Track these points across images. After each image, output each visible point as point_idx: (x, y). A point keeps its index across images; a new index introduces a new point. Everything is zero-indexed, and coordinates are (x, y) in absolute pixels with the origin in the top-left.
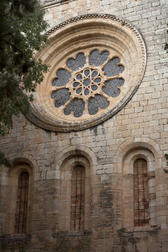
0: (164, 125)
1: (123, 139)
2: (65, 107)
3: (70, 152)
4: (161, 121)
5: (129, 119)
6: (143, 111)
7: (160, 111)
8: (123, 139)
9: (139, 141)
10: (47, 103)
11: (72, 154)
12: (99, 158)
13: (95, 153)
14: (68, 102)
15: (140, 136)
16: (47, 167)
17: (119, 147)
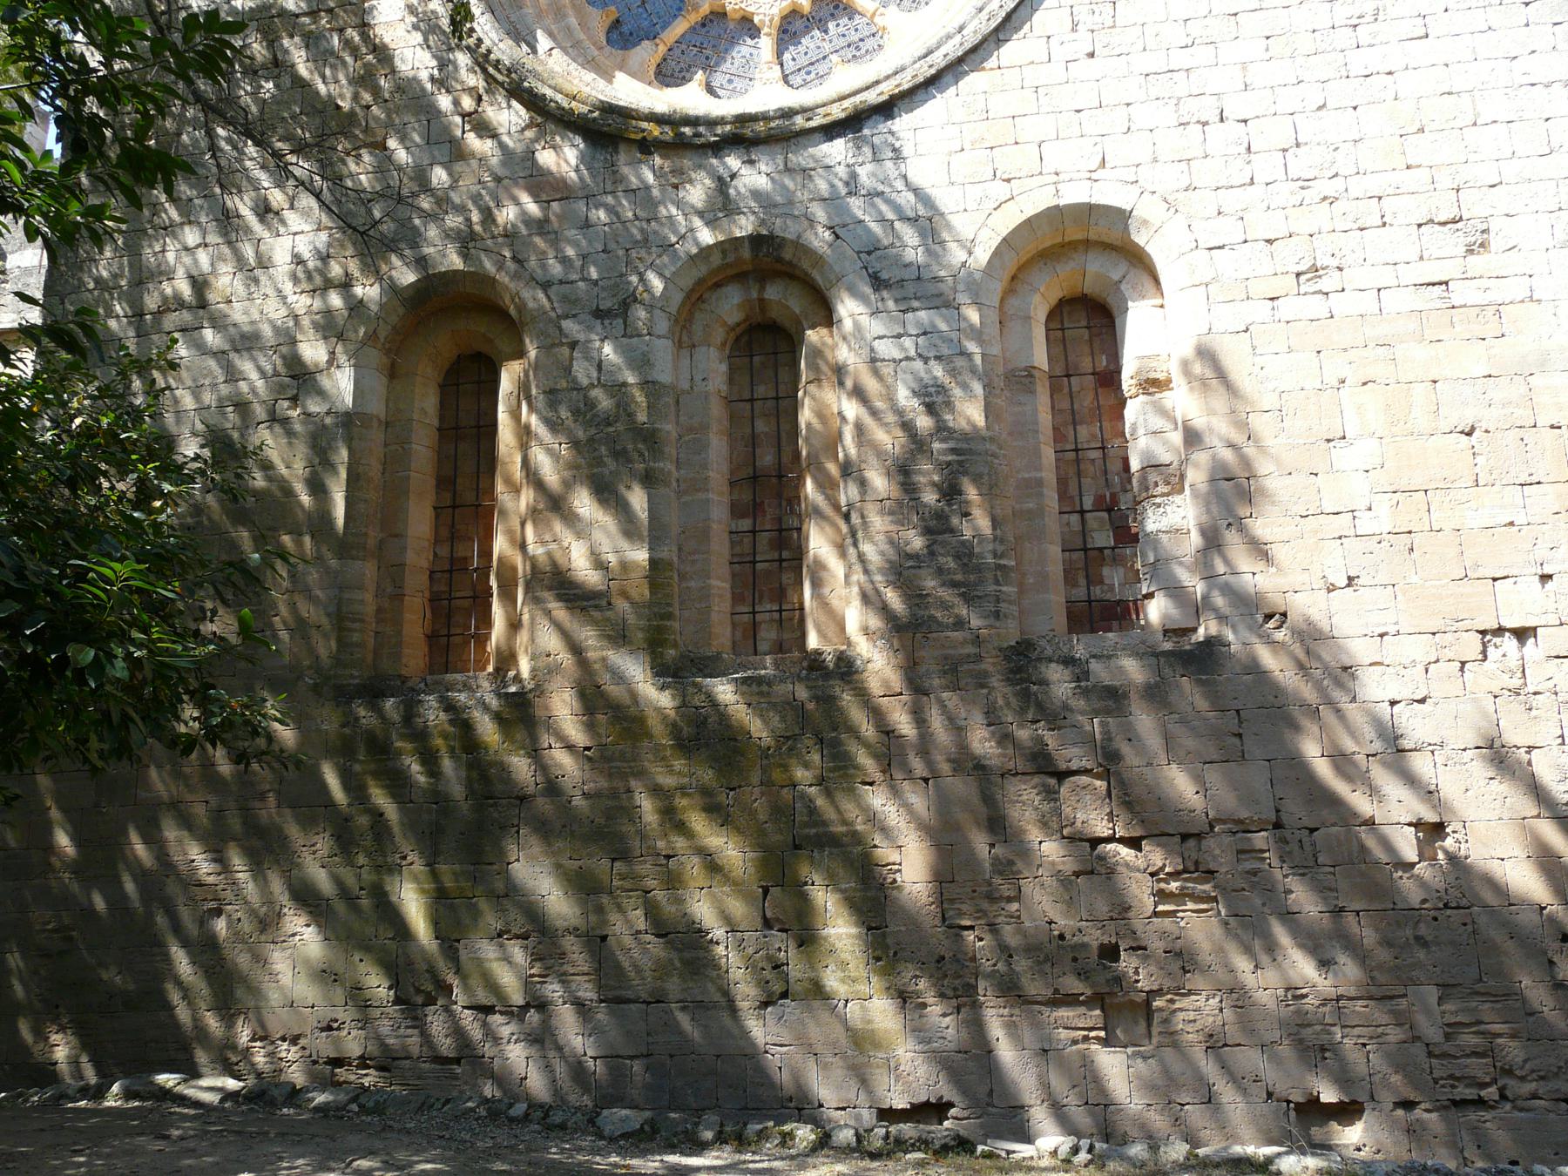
0: (1205, 124)
1: (1000, 190)
2: (662, 49)
3: (727, 246)
4: (1193, 109)
5: (1029, 93)
6: (1092, 55)
7: (1180, 59)
8: (1000, 190)
9: (1086, 200)
10: (573, 21)
11: (731, 258)
12: (884, 275)
13: (859, 253)
14: (680, 27)
15: (1088, 175)
16: (607, 322)
17: (984, 224)
